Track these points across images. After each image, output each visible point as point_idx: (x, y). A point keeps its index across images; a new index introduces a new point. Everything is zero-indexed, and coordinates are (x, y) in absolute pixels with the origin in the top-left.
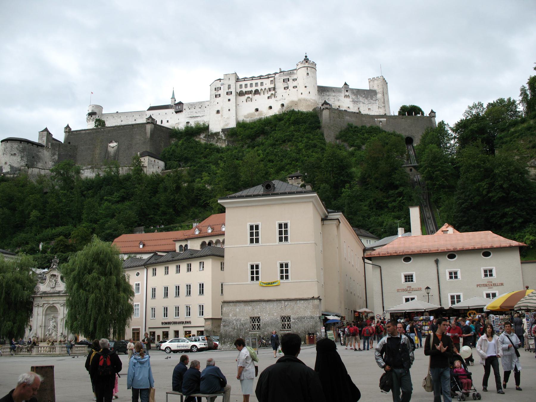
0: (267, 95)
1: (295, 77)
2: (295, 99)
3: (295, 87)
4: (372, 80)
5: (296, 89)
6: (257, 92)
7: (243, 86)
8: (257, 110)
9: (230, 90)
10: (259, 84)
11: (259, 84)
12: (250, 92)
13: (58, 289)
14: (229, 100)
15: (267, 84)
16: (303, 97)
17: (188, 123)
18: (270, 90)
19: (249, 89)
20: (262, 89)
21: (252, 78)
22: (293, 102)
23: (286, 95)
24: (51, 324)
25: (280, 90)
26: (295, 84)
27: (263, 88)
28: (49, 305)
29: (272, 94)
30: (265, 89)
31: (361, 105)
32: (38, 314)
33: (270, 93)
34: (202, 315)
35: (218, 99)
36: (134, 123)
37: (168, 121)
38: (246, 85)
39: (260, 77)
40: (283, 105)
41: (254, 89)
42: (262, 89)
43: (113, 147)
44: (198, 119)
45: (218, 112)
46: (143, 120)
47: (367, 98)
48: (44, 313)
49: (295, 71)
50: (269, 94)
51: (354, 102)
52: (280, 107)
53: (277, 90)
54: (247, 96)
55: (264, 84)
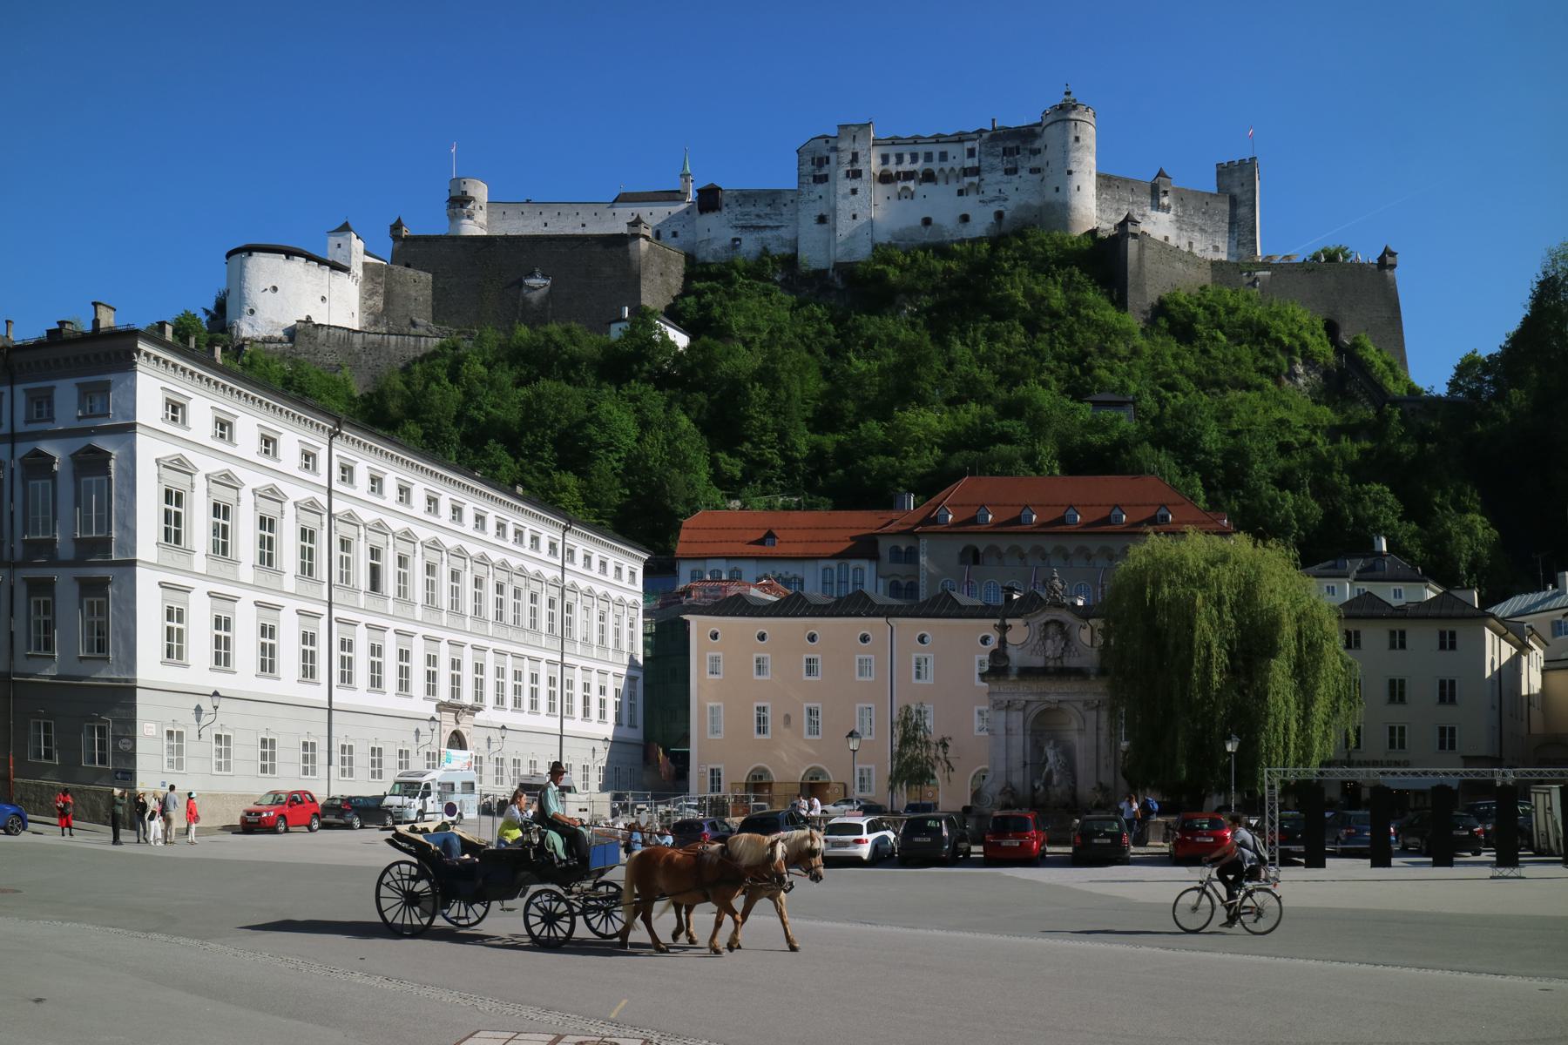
0: (954, 187)
1: (1037, 144)
2: (1035, 201)
3: (1034, 171)
4: (1224, 171)
5: (1037, 177)
6: (929, 177)
7: (893, 160)
8: (927, 222)
9: (857, 167)
10: (936, 156)
11: (936, 156)
12: (909, 176)
13: (1072, 662)
14: (854, 192)
15: (958, 157)
16: (1058, 197)
17: (734, 240)
18: (967, 172)
19: (907, 166)
20: (942, 170)
21: (916, 140)
22: (1028, 207)
23: (1008, 189)
24: (1051, 759)
25: (994, 180)
26: (1035, 162)
27: (947, 166)
28: (1044, 707)
29: (971, 184)
30: (952, 169)
31: (1197, 235)
32: (1008, 730)
33: (967, 180)
34: (1452, 746)
35: (820, 188)
36: (579, 231)
37: (675, 234)
38: (900, 159)
39: (938, 139)
40: (999, 215)
41: (919, 166)
42: (942, 170)
43: (535, 289)
44: (768, 234)
45: (822, 219)
46: (622, 229)
47: (1211, 217)
48: (1028, 726)
49: (1038, 129)
50: (959, 186)
51: (1180, 222)
52: (992, 219)
53: (985, 176)
54: (900, 185)
55: (950, 157)
